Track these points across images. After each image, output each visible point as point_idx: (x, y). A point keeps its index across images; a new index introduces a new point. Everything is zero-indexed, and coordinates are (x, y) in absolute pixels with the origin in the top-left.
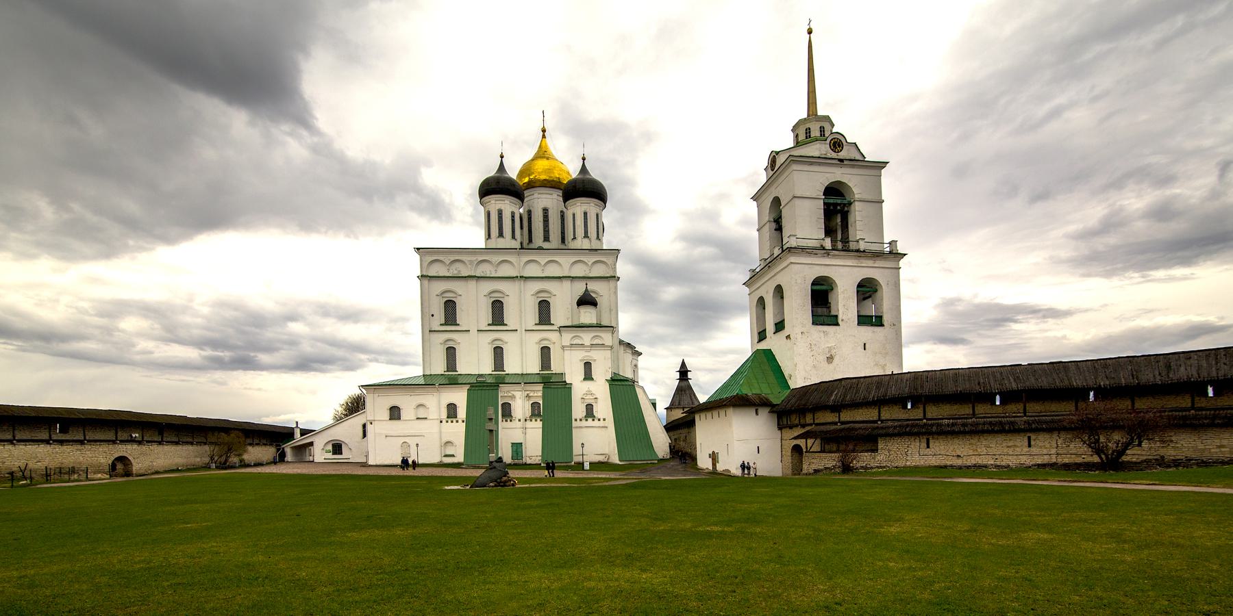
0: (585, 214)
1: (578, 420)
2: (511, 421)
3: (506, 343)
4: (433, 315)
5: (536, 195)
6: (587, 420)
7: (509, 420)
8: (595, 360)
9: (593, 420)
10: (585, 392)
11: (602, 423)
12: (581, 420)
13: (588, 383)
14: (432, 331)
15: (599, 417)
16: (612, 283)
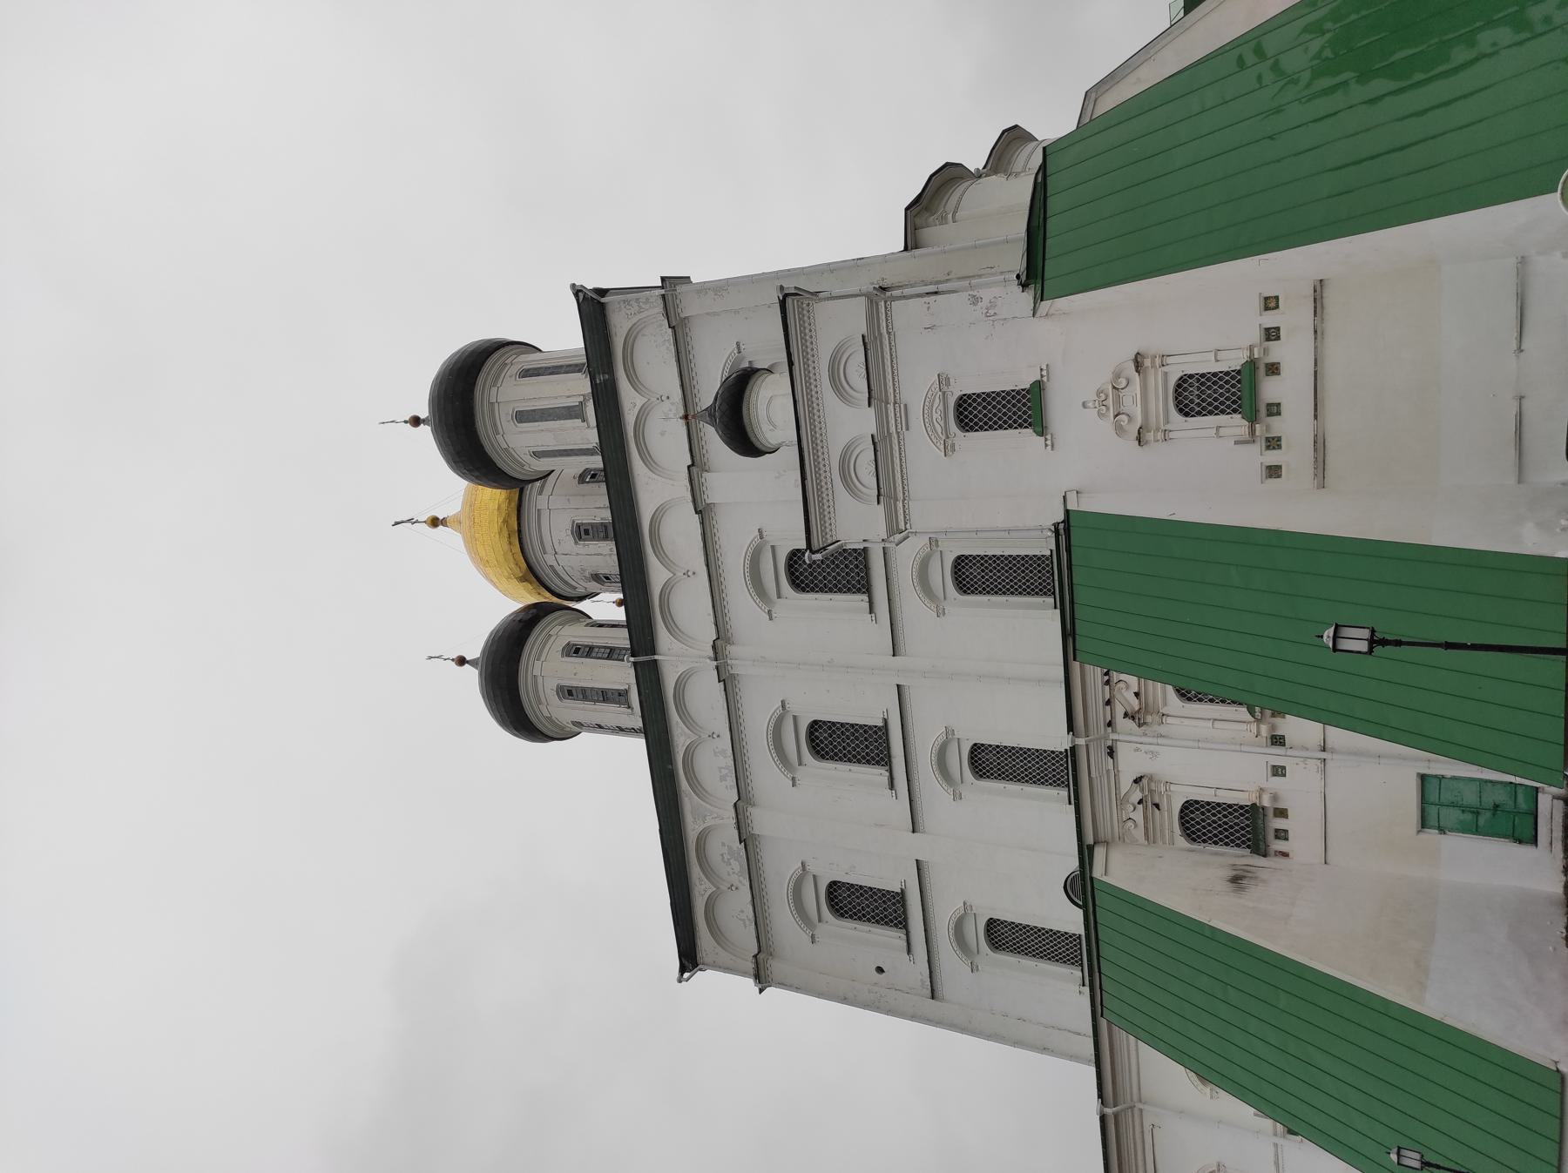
0: (522, 417)
1: (1272, 458)
2: (1282, 813)
3: (949, 732)
4: (880, 970)
5: (550, 559)
6: (1274, 409)
7: (1279, 823)
8: (943, 380)
9: (1273, 369)
10: (1107, 425)
11: (1294, 318)
12: (1273, 443)
13: (1058, 407)
14: (933, 991)
15: (1255, 336)
16: (690, 307)
